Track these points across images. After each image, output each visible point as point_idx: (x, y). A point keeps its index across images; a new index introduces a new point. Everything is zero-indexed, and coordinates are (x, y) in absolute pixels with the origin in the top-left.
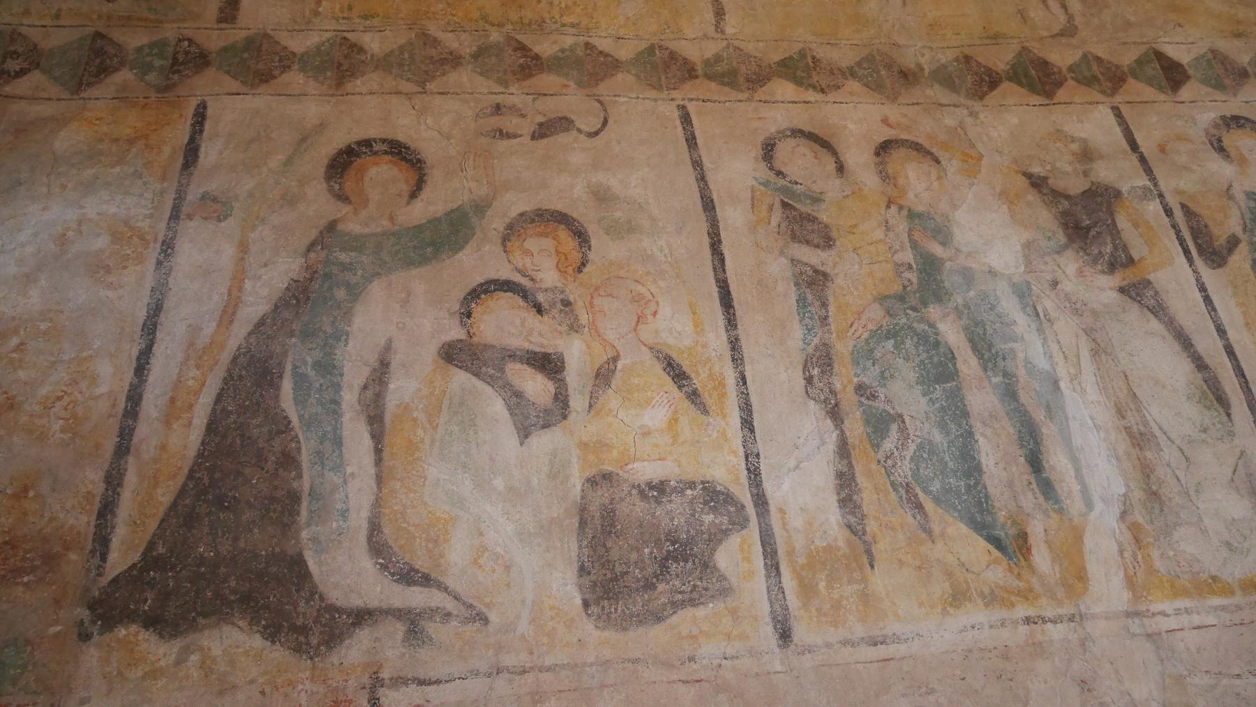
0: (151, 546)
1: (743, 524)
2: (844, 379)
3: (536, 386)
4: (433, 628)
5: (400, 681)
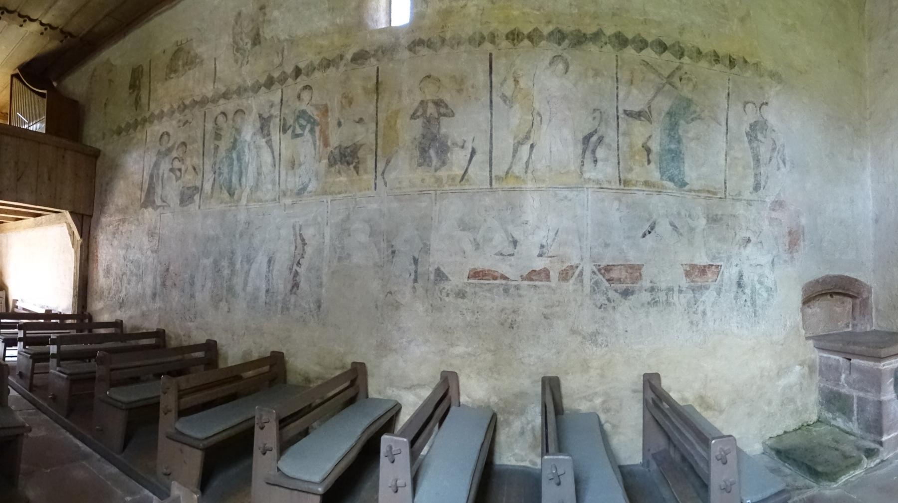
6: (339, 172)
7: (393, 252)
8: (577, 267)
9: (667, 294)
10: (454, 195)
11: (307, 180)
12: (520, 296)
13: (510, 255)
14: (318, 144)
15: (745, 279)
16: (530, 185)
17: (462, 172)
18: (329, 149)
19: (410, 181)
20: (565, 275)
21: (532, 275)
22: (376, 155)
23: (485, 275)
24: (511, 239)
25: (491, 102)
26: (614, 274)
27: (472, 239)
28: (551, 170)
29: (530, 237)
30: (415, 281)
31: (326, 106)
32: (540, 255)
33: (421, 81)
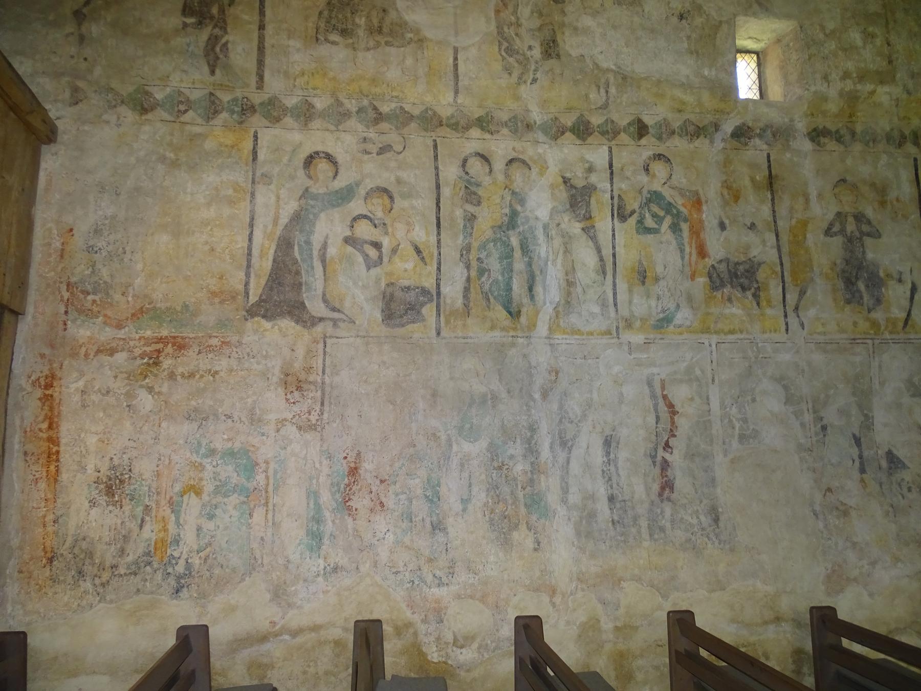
0: (261, 295)
1: (432, 301)
2: (473, 256)
3: (373, 253)
4: (341, 324)
5: (331, 337)
7: (824, 428)
11: (672, 306)
14: (687, 250)
19: (838, 325)
22: (783, 282)
33: (835, 186)
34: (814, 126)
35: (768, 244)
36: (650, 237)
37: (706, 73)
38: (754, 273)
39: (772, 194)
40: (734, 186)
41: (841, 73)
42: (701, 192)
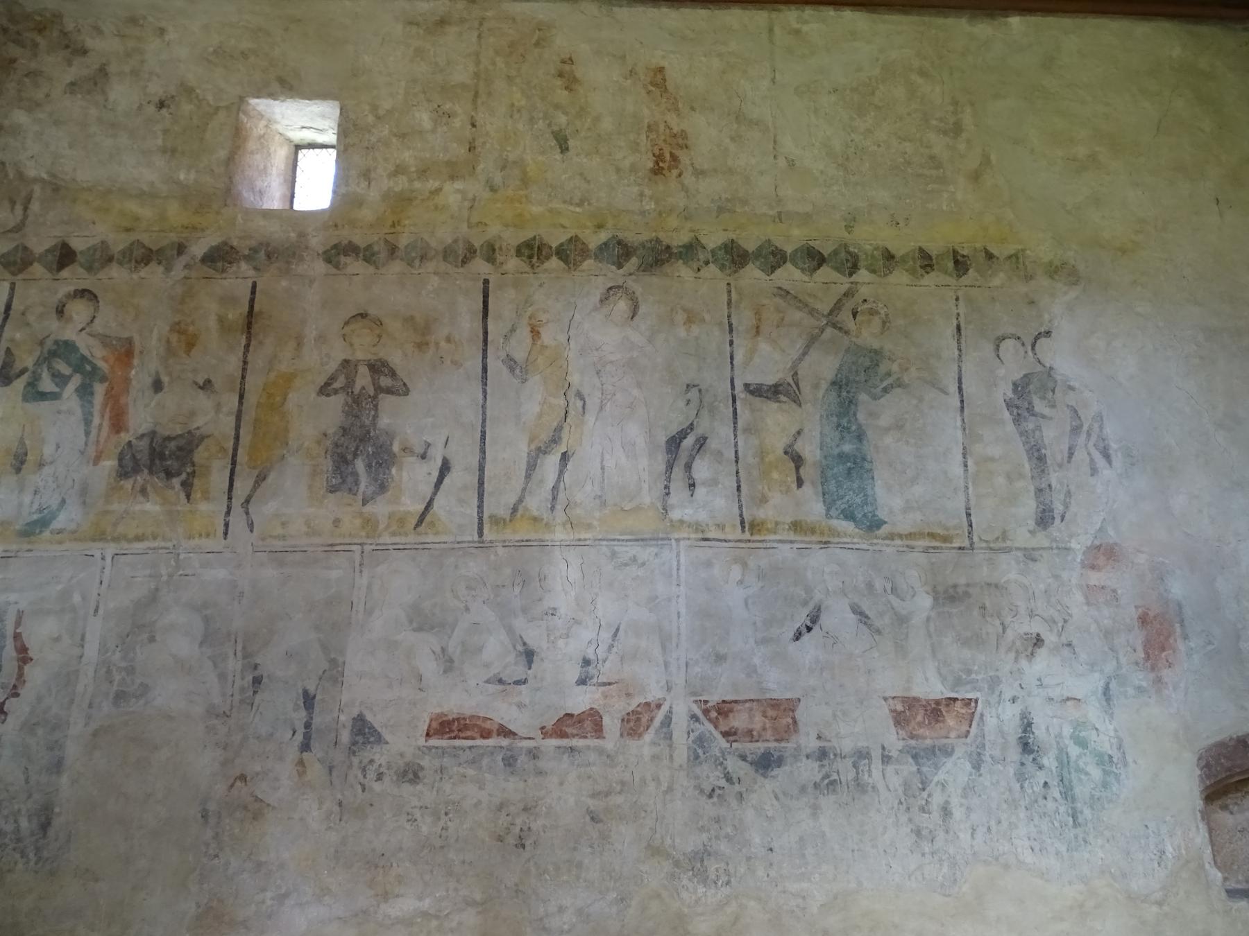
6: (143, 491)
8: (659, 706)
9: (855, 766)
10: (401, 554)
12: (540, 773)
13: (517, 683)
14: (96, 421)
15: (1039, 732)
16: (560, 535)
17: (421, 507)
18: (125, 437)
20: (634, 724)
21: (566, 725)
22: (234, 463)
23: (466, 727)
24: (520, 648)
25: (485, 369)
26: (738, 721)
27: (438, 650)
28: (604, 504)
29: (561, 643)
30: (306, 747)
31: (130, 341)
32: (582, 682)
33: (347, 323)
34: (334, 241)
35: (225, 409)
36: (45, 405)
37: (182, 177)
38: (191, 451)
39: (249, 339)
40: (191, 328)
41: (391, 168)
42: (137, 338)
